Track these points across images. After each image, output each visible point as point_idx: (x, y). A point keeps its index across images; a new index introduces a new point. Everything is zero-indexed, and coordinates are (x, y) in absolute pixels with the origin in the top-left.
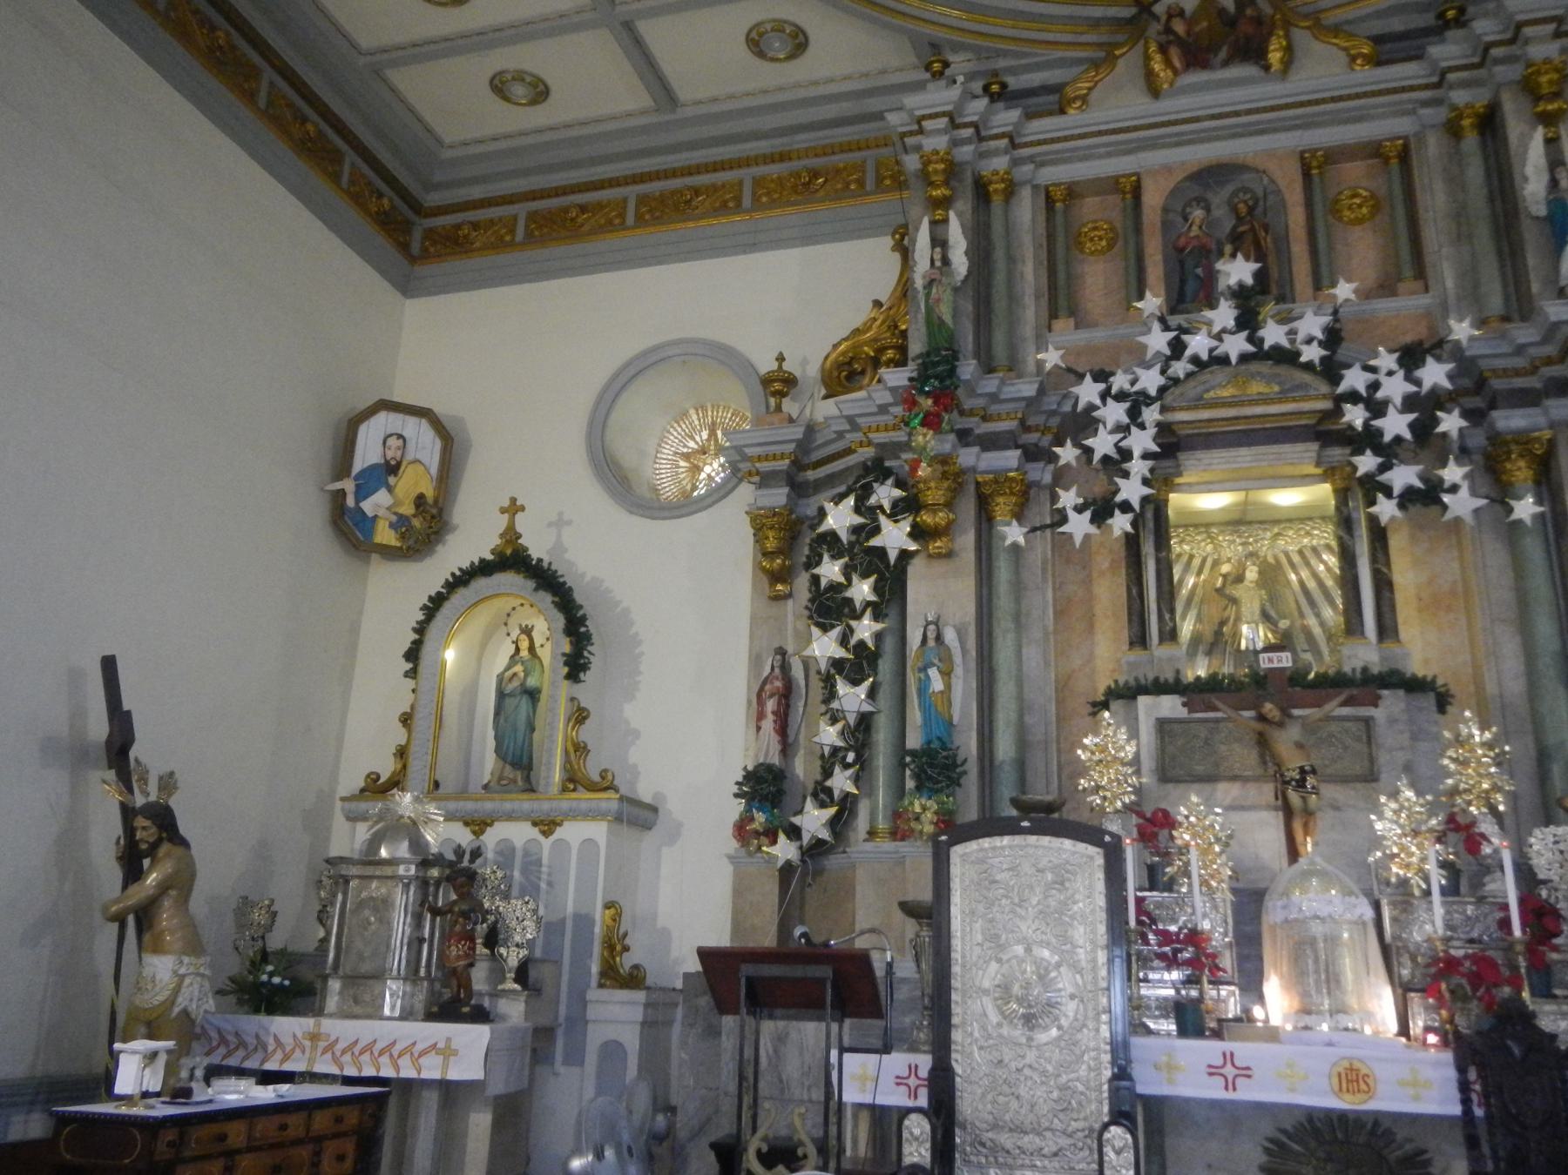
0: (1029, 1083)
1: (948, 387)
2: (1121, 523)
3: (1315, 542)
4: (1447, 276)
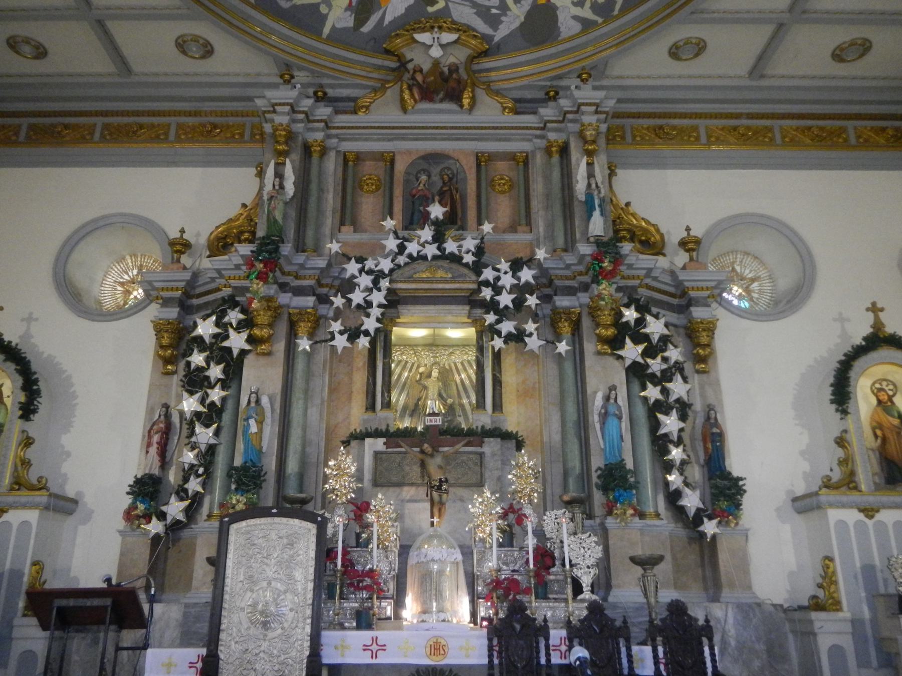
0: (262, 662)
1: (273, 258)
2: (363, 342)
3: (469, 358)
4: (541, 226)
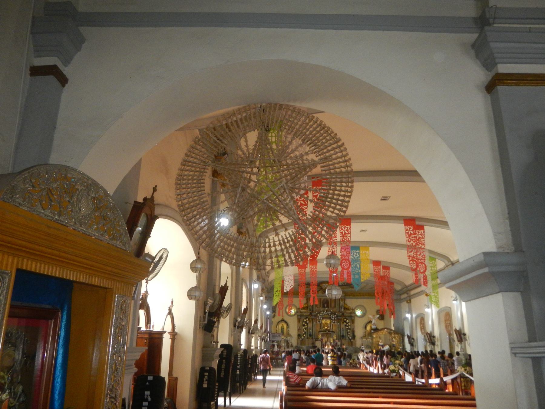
4: (337, 308)
